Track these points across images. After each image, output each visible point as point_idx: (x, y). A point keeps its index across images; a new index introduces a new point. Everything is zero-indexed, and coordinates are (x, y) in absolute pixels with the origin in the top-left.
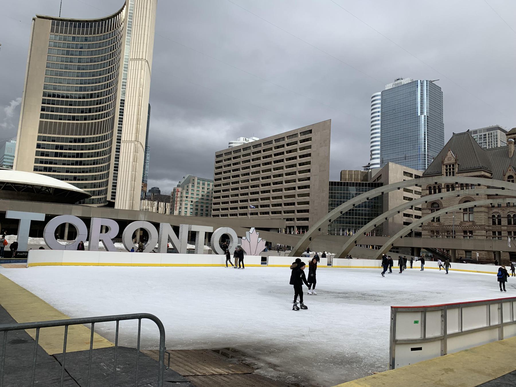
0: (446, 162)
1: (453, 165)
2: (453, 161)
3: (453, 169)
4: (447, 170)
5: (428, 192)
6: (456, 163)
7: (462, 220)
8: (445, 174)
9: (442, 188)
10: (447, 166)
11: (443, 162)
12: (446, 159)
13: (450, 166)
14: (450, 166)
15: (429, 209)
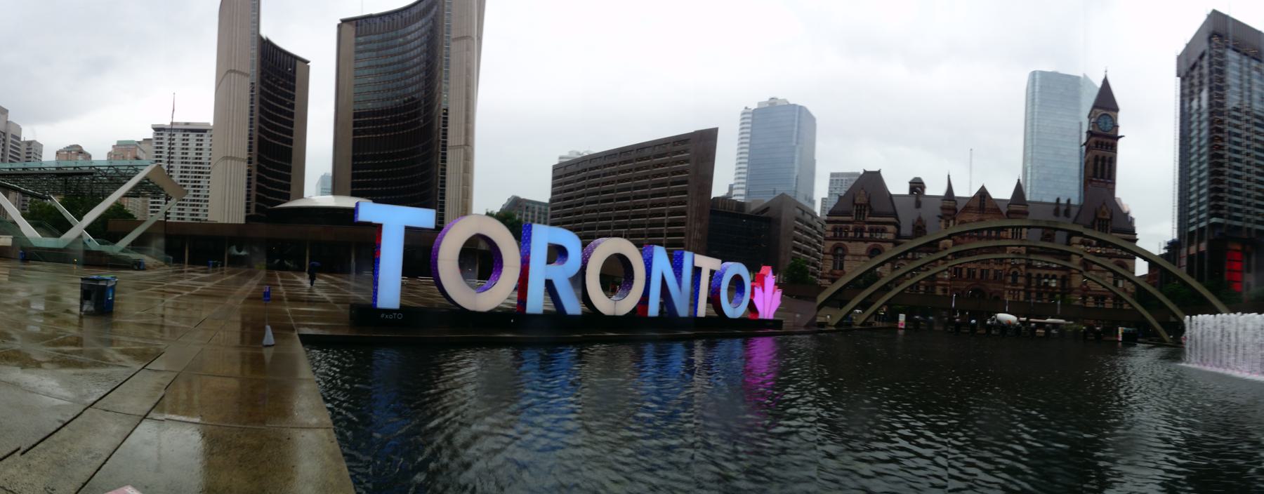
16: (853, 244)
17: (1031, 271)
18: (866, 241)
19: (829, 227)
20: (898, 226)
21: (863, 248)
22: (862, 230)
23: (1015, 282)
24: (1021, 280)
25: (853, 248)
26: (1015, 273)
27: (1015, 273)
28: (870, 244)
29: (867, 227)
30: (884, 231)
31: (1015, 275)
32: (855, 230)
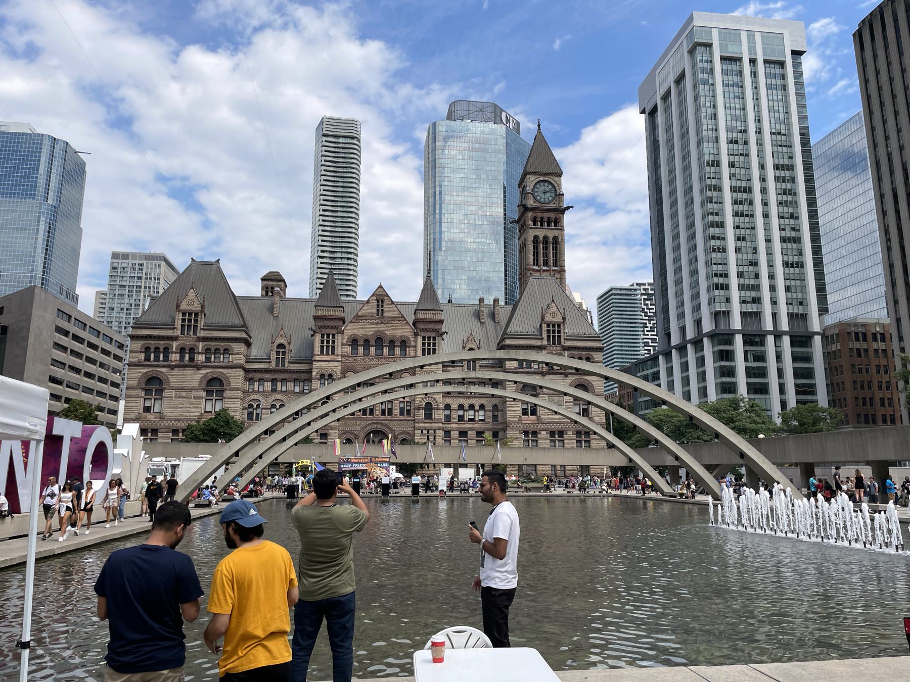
0: (184, 307)
1: (196, 314)
2: (197, 307)
3: (196, 321)
4: (183, 320)
5: (142, 356)
6: (202, 311)
7: (203, 412)
8: (180, 327)
9: (173, 353)
10: (184, 314)
11: (178, 306)
12: (184, 302)
13: (190, 314)
14: (190, 314)
15: (142, 389)
16: (176, 371)
17: (449, 401)
18: (198, 368)
19: (138, 345)
20: (248, 344)
21: (194, 378)
22: (192, 351)
23: (429, 416)
24: (437, 414)
25: (175, 377)
26: (429, 404)
27: (428, 404)
28: (204, 372)
29: (201, 346)
30: (227, 351)
31: (429, 408)
32: (182, 351)
